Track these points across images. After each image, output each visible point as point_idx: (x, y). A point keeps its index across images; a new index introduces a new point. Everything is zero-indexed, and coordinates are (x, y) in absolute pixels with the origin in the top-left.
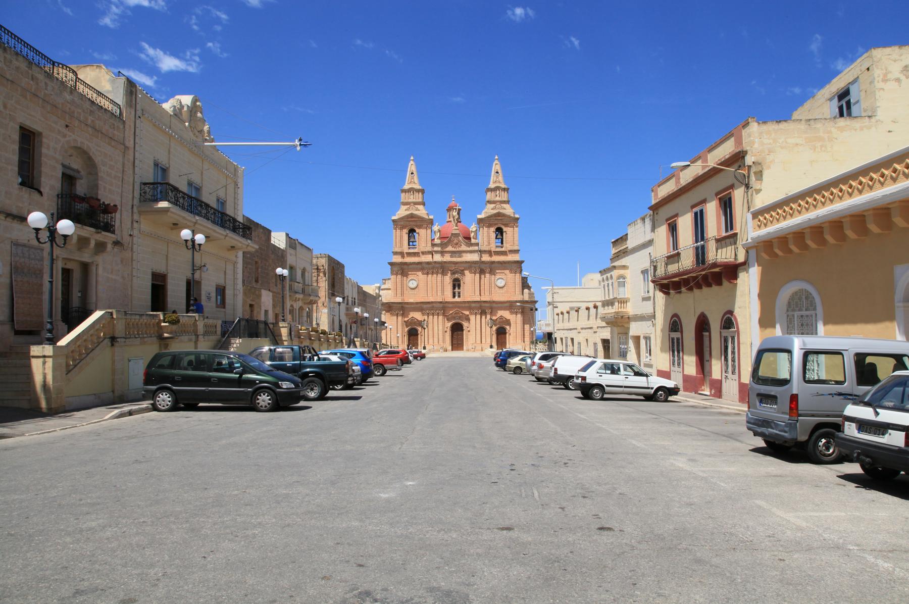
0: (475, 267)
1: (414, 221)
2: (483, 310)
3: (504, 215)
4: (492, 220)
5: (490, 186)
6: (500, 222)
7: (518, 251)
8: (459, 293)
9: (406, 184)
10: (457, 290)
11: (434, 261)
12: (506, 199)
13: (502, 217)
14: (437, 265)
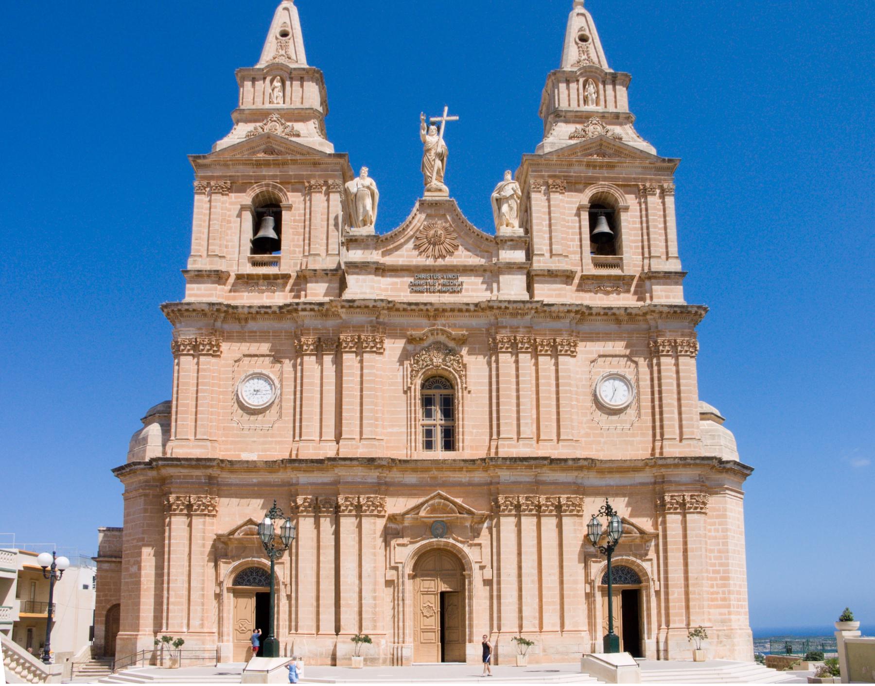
0: (515, 329)
4: (576, 168)
6: (606, 173)
13: (610, 156)
14: (359, 318)
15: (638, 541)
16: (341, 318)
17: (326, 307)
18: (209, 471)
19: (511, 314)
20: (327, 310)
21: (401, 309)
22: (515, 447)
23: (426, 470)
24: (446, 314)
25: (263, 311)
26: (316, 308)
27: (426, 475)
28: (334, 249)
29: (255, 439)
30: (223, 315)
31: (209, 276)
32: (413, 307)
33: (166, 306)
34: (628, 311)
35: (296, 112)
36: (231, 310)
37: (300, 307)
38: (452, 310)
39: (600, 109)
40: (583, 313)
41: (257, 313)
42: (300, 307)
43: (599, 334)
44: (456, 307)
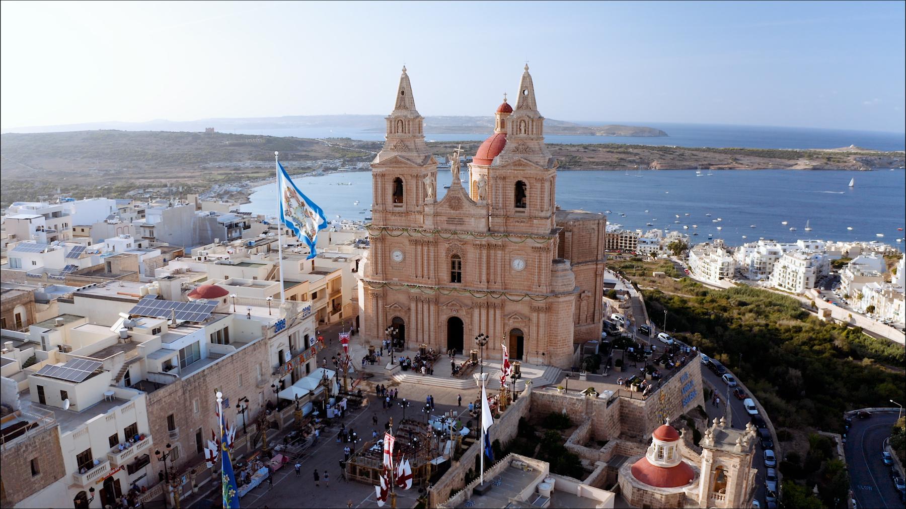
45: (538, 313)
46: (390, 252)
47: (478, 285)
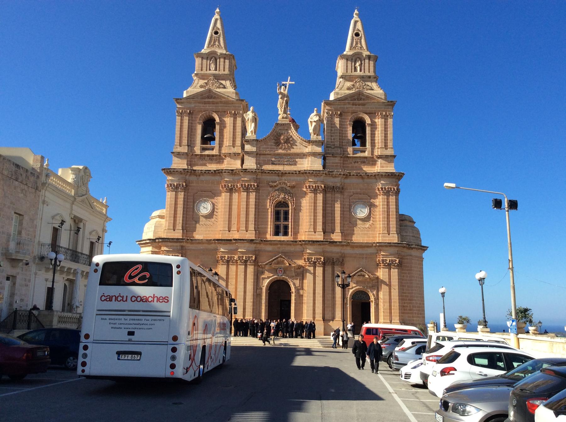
1: (213, 103)
2: (328, 259)
3: (368, 97)
4: (348, 106)
5: (345, 53)
7: (394, 156)
8: (286, 227)
9: (205, 47)
10: (282, 223)
11: (243, 168)
12: (372, 74)
15: (368, 280)
16: (241, 176)
17: (234, 171)
18: (182, 244)
19: (314, 175)
20: (235, 172)
21: (267, 172)
22: (315, 235)
23: (277, 244)
24: (286, 175)
25: (207, 172)
26: (230, 171)
27: (276, 247)
28: (238, 144)
29: (202, 229)
30: (189, 173)
31: (183, 155)
32: (272, 172)
33: (164, 169)
34: (367, 174)
35: (222, 75)
36: (193, 171)
37: (223, 171)
38: (289, 173)
39: (362, 74)
40: (347, 175)
41: (205, 173)
42: (223, 171)
43: (354, 184)
44: (291, 172)
45: (390, 269)
46: (194, 203)
47: (311, 235)
